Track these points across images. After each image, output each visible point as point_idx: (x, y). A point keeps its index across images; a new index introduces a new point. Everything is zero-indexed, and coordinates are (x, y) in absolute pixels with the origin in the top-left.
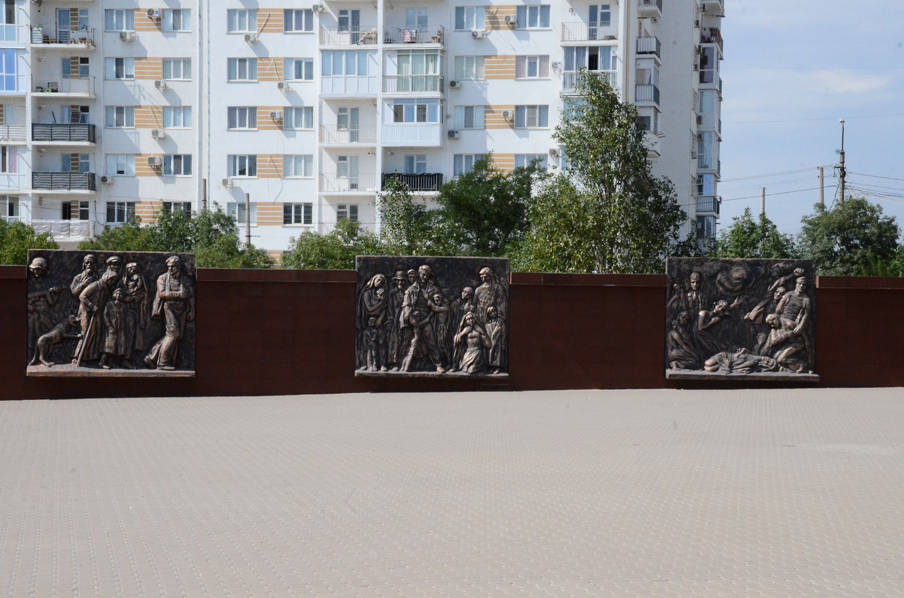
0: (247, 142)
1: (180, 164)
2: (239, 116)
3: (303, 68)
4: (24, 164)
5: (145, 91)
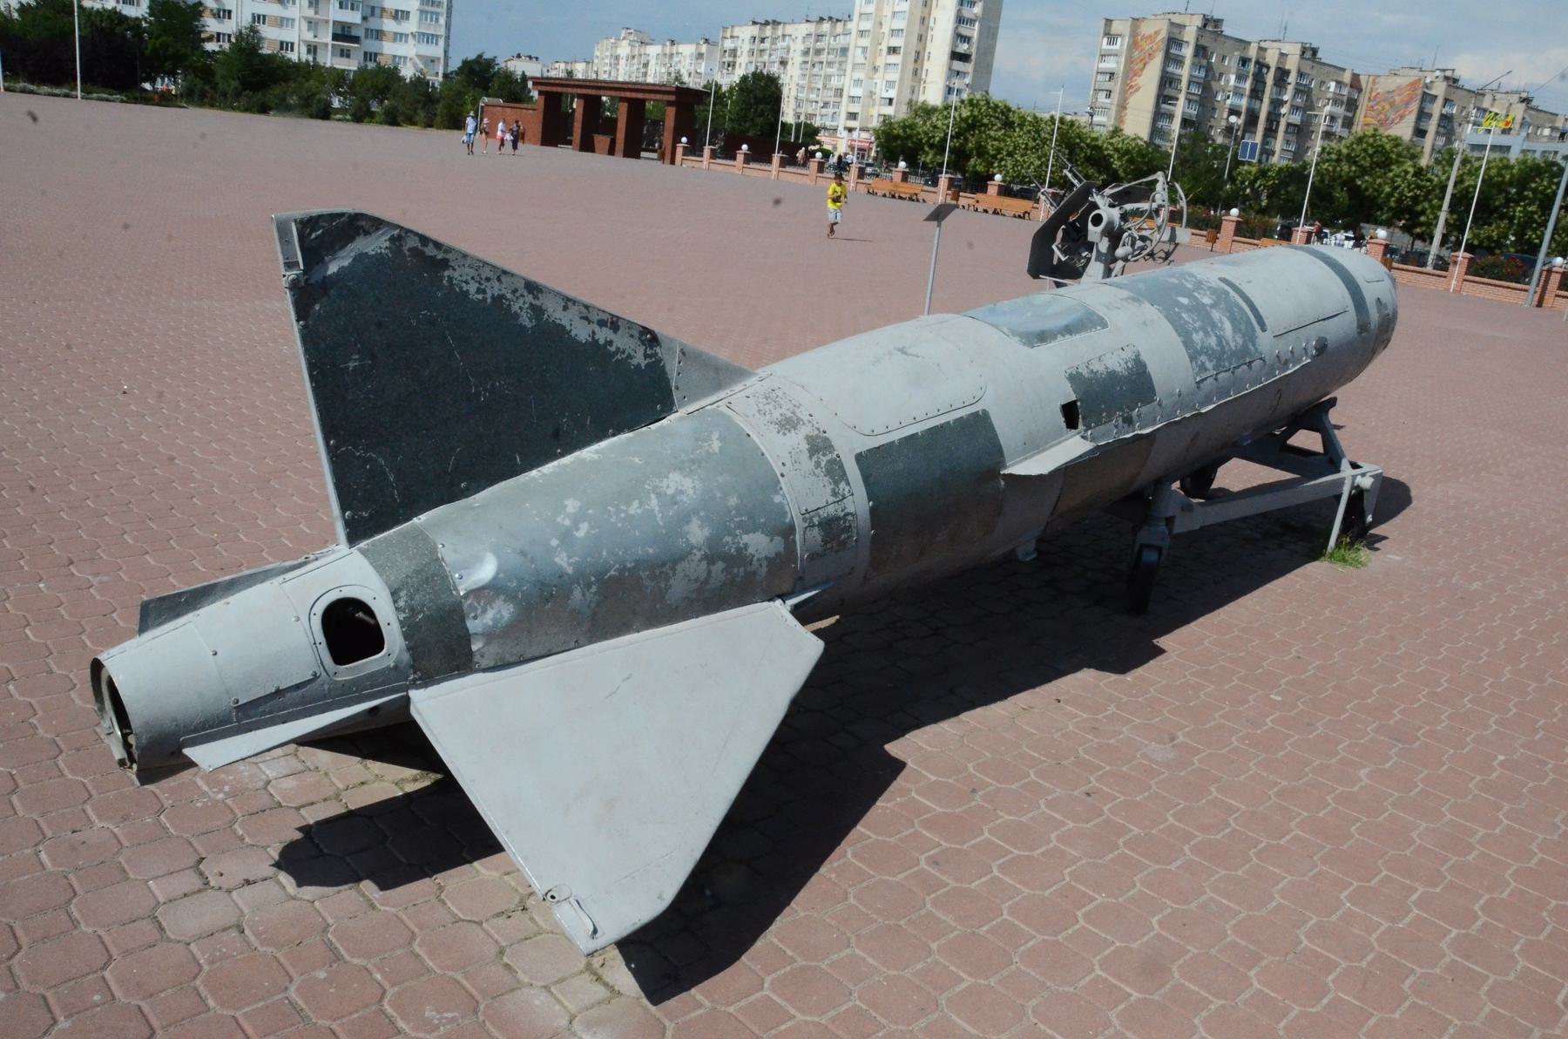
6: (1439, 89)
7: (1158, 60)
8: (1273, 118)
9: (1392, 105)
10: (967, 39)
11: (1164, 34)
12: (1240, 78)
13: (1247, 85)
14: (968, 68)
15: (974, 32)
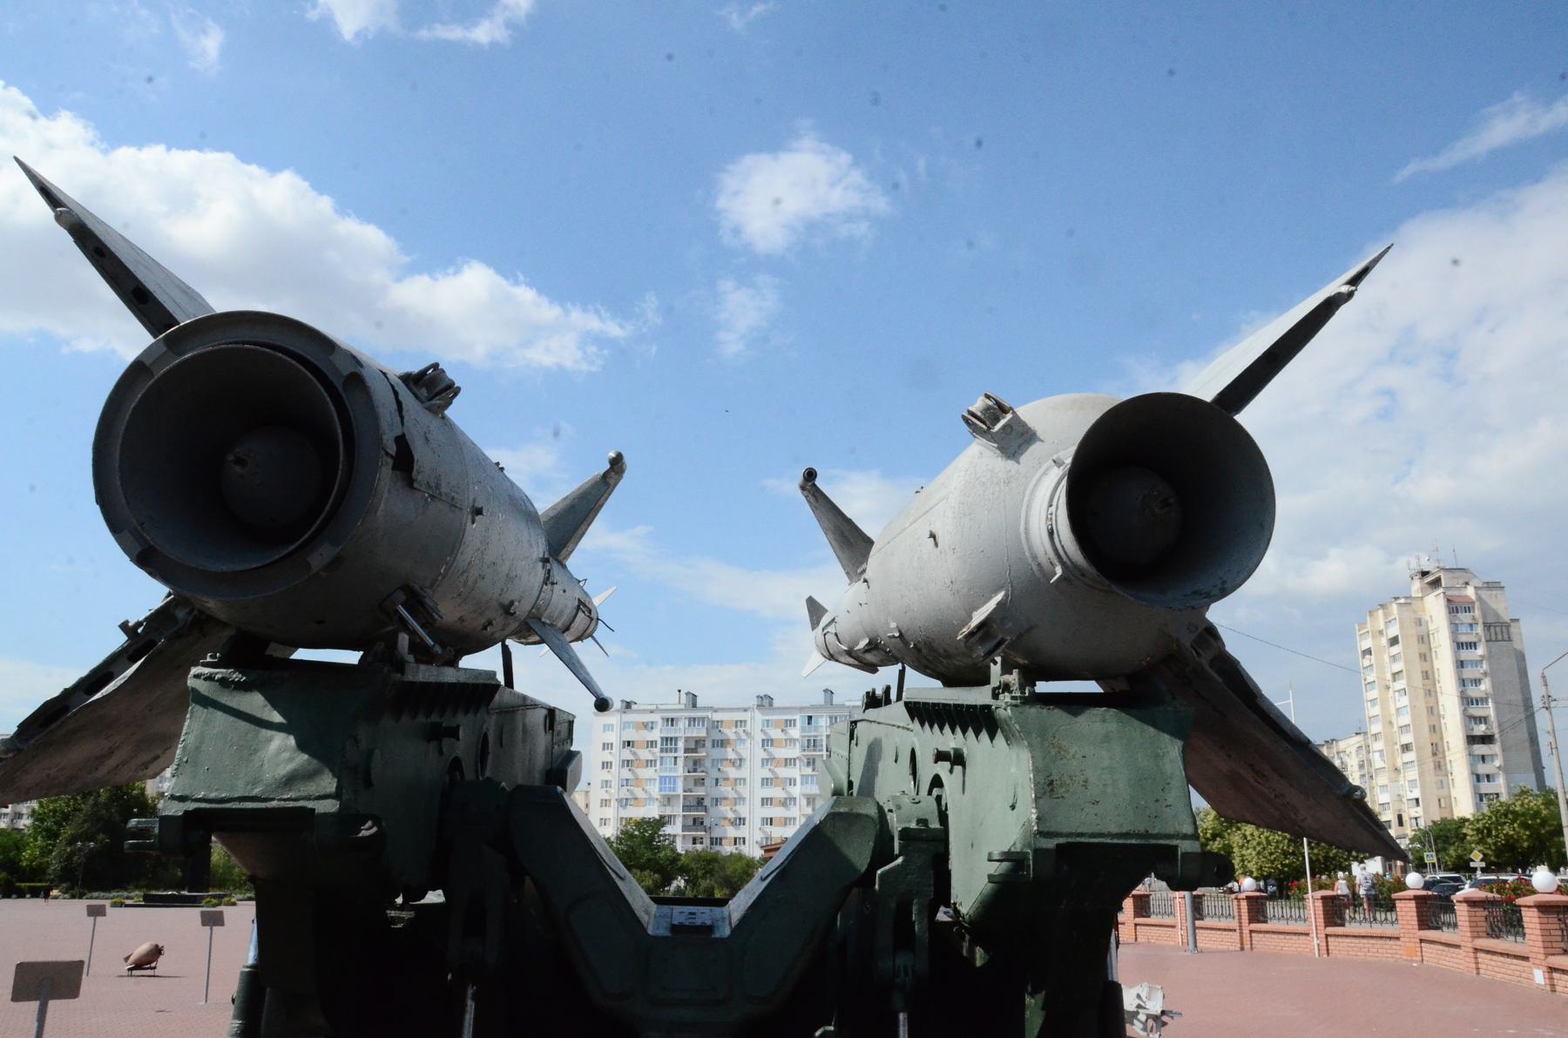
0: (770, 812)
1: (740, 821)
2: (766, 801)
3: (792, 782)
4: (679, 822)
5: (726, 790)
10: (1483, 720)
14: (1496, 748)
15: (1490, 710)
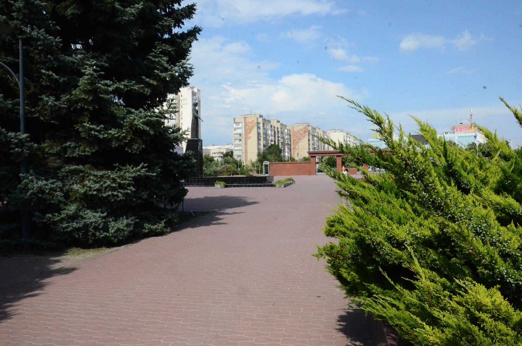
6: (310, 128)
7: (256, 128)
8: (279, 140)
9: (300, 134)
11: (256, 121)
12: (271, 131)
13: (273, 133)
